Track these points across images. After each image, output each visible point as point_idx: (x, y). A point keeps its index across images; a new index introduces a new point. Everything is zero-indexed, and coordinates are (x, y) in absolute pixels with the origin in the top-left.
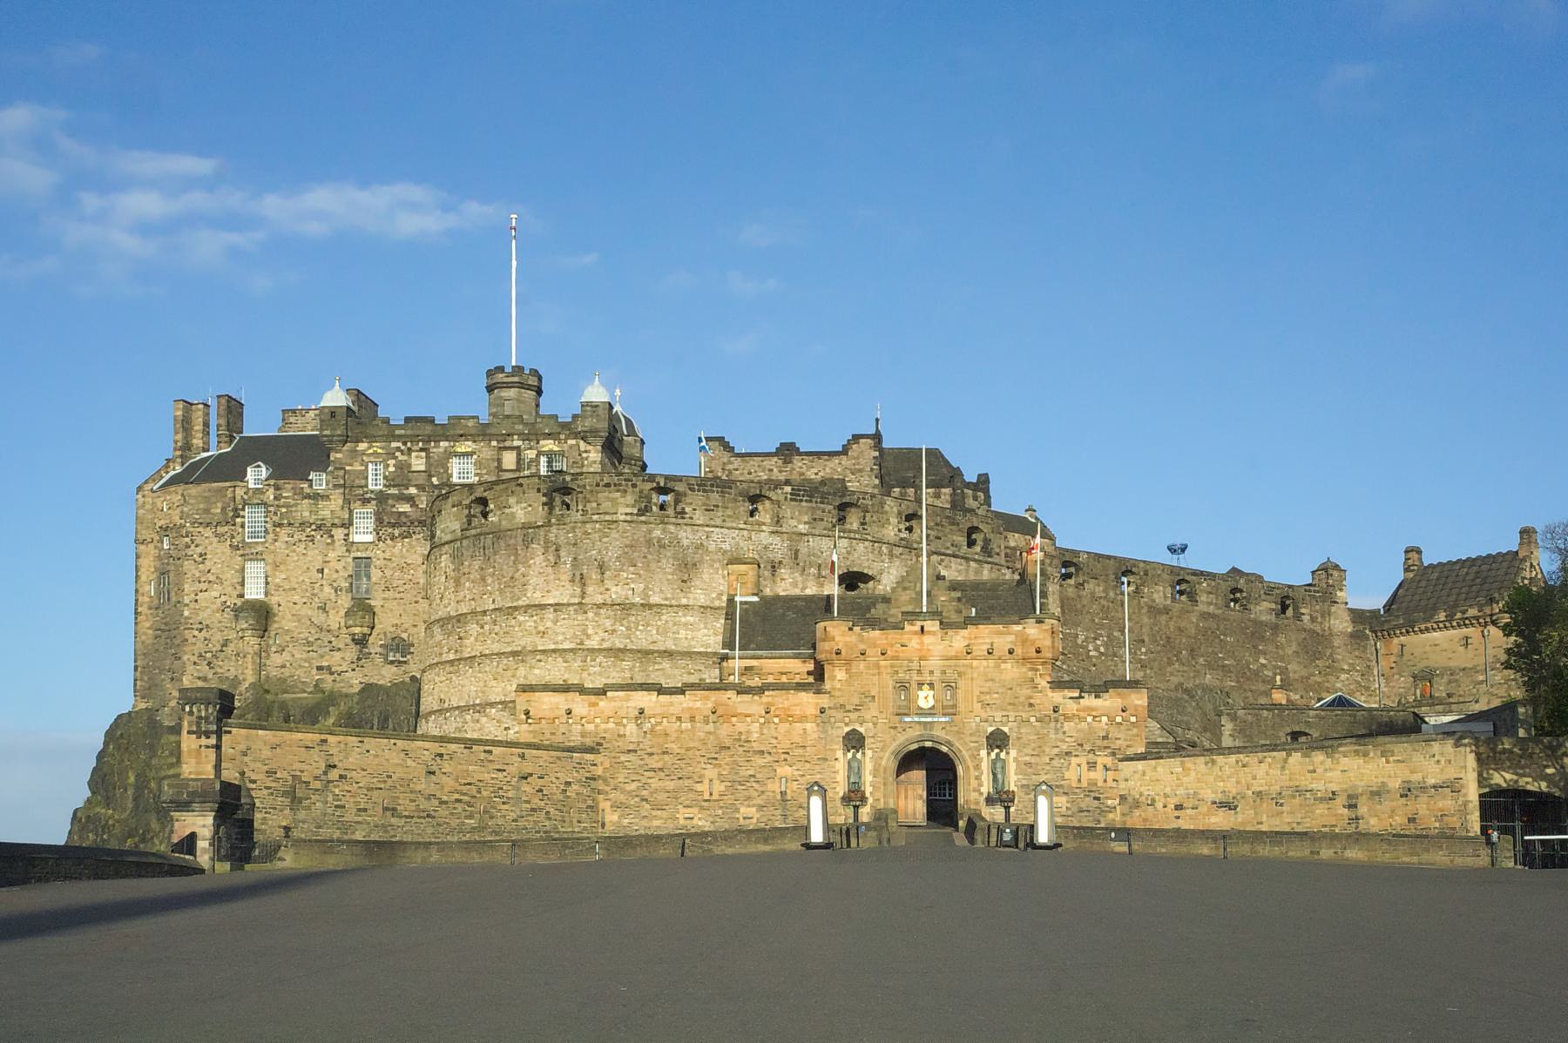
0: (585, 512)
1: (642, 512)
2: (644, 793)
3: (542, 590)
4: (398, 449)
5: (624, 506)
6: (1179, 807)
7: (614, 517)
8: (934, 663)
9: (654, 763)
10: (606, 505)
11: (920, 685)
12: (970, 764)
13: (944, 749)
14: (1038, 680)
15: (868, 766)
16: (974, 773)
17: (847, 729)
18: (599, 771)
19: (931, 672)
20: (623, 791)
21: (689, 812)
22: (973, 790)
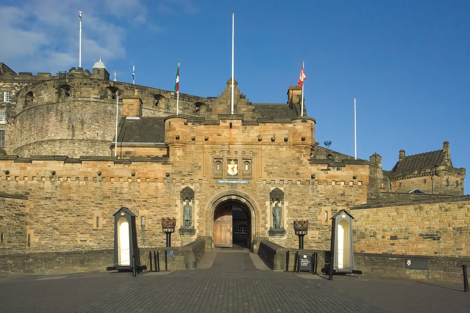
0: (74, 96)
1: (102, 98)
2: (56, 224)
3: (55, 133)
4: (16, 86)
5: (94, 94)
6: (394, 238)
7: (89, 99)
8: (238, 147)
9: (62, 206)
10: (85, 94)
11: (229, 160)
12: (259, 210)
13: (244, 201)
14: (302, 158)
15: (196, 210)
16: (262, 216)
17: (183, 187)
18: (27, 210)
19: (236, 152)
20: (42, 223)
21: (83, 237)
22: (261, 227)
